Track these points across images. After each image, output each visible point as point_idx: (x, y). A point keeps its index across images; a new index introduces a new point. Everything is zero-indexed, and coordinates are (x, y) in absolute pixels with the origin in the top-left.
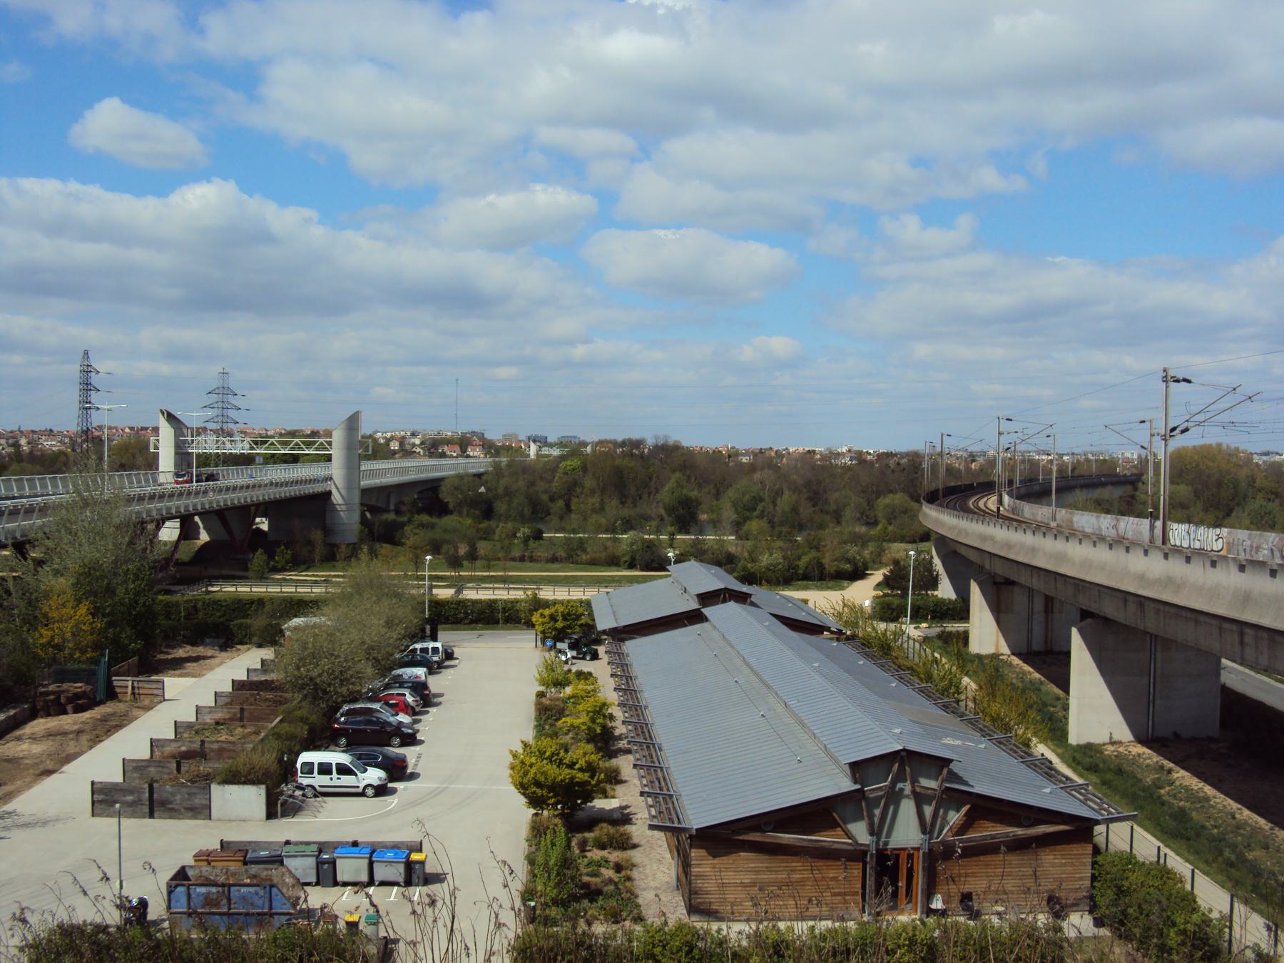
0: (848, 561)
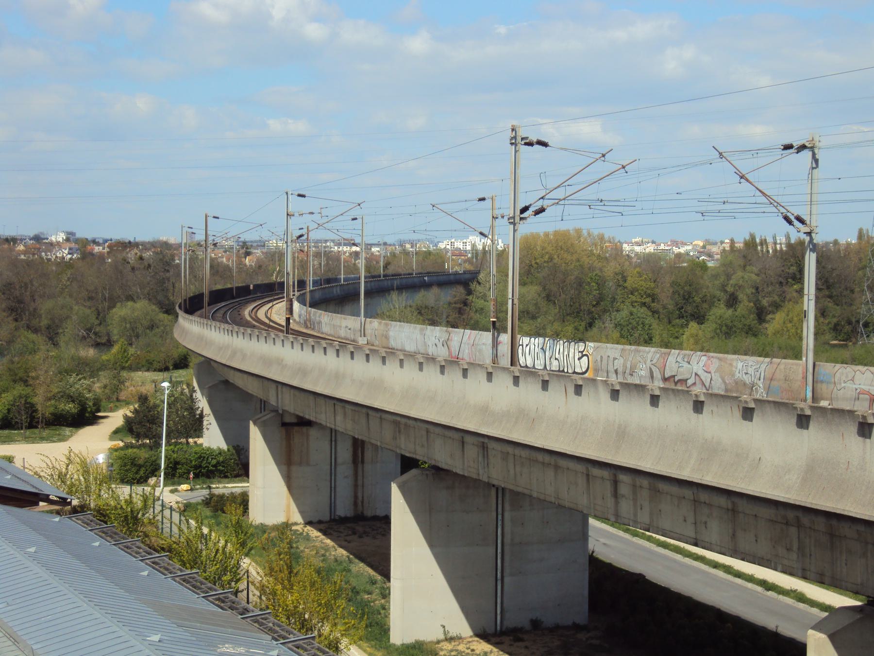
0: (71, 399)
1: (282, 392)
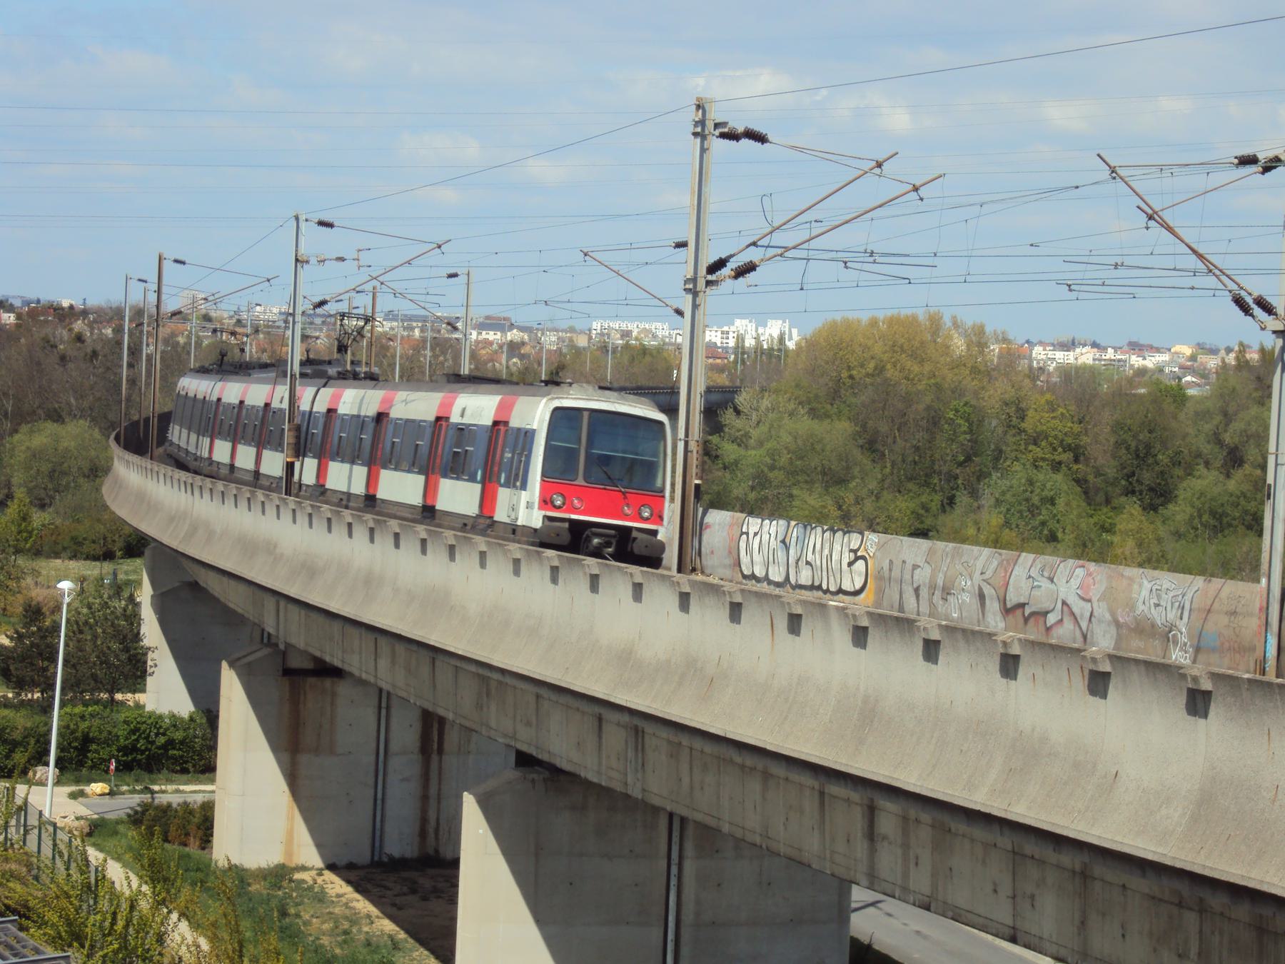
1: (286, 608)
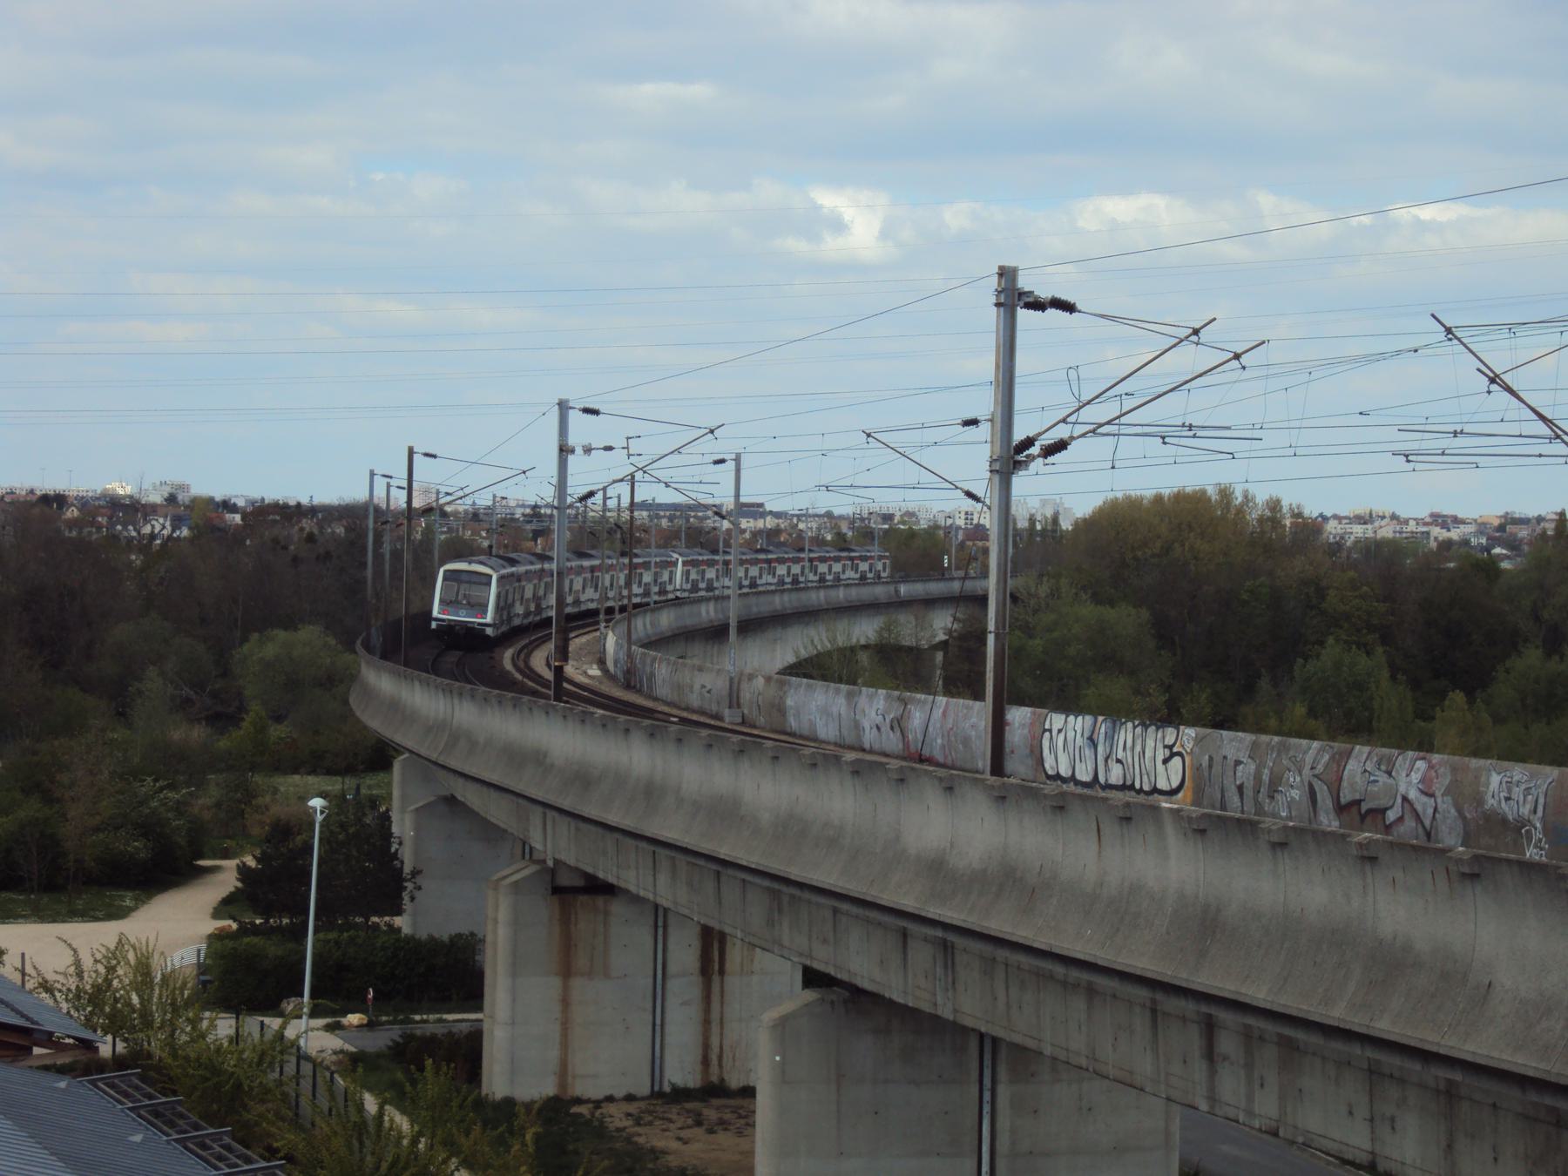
1: (554, 821)
